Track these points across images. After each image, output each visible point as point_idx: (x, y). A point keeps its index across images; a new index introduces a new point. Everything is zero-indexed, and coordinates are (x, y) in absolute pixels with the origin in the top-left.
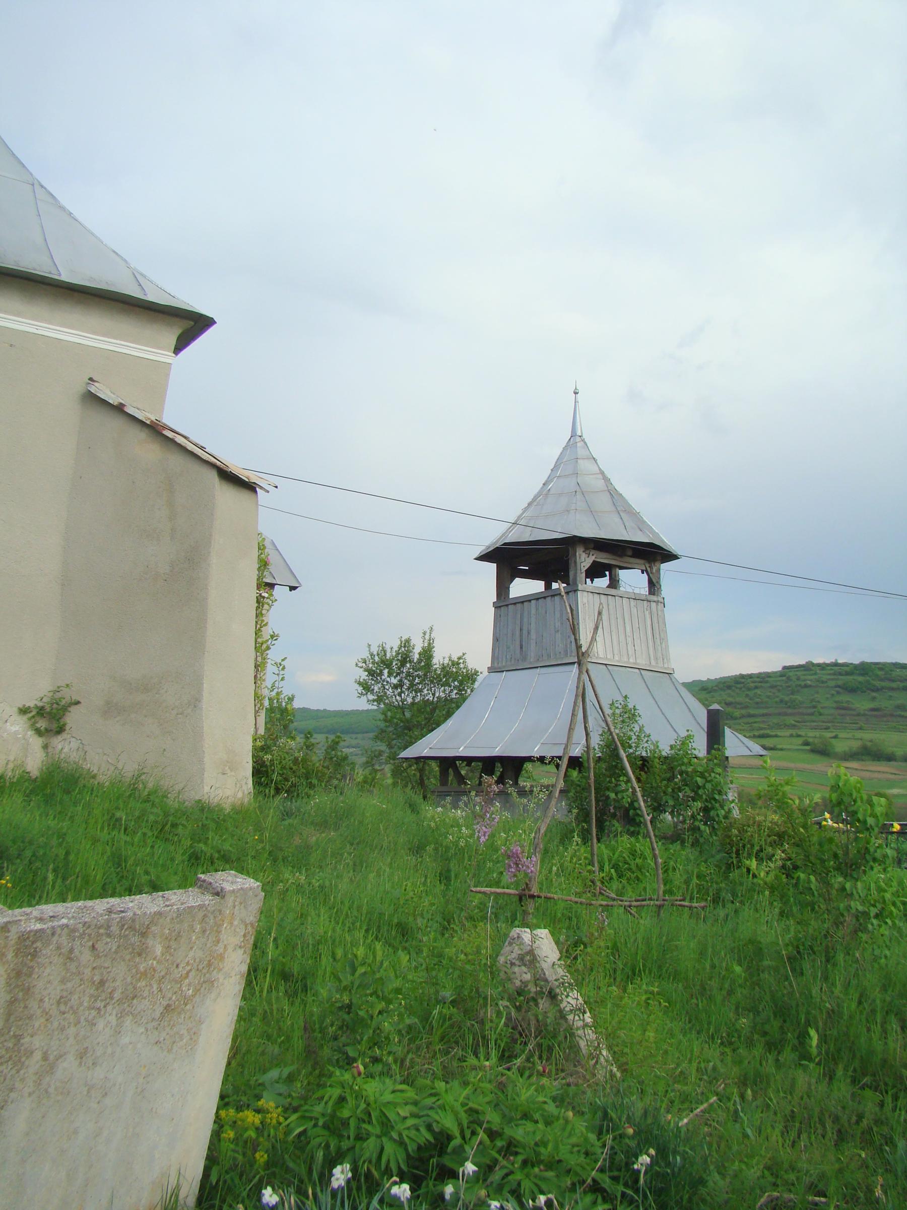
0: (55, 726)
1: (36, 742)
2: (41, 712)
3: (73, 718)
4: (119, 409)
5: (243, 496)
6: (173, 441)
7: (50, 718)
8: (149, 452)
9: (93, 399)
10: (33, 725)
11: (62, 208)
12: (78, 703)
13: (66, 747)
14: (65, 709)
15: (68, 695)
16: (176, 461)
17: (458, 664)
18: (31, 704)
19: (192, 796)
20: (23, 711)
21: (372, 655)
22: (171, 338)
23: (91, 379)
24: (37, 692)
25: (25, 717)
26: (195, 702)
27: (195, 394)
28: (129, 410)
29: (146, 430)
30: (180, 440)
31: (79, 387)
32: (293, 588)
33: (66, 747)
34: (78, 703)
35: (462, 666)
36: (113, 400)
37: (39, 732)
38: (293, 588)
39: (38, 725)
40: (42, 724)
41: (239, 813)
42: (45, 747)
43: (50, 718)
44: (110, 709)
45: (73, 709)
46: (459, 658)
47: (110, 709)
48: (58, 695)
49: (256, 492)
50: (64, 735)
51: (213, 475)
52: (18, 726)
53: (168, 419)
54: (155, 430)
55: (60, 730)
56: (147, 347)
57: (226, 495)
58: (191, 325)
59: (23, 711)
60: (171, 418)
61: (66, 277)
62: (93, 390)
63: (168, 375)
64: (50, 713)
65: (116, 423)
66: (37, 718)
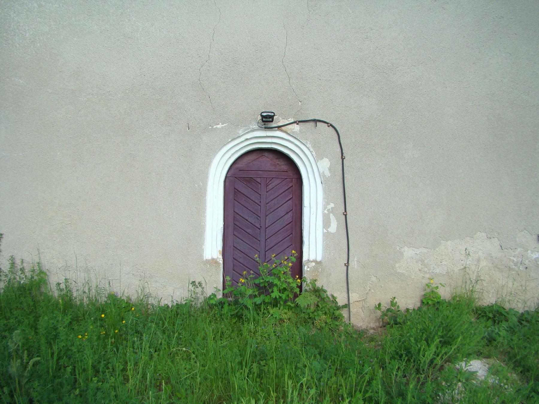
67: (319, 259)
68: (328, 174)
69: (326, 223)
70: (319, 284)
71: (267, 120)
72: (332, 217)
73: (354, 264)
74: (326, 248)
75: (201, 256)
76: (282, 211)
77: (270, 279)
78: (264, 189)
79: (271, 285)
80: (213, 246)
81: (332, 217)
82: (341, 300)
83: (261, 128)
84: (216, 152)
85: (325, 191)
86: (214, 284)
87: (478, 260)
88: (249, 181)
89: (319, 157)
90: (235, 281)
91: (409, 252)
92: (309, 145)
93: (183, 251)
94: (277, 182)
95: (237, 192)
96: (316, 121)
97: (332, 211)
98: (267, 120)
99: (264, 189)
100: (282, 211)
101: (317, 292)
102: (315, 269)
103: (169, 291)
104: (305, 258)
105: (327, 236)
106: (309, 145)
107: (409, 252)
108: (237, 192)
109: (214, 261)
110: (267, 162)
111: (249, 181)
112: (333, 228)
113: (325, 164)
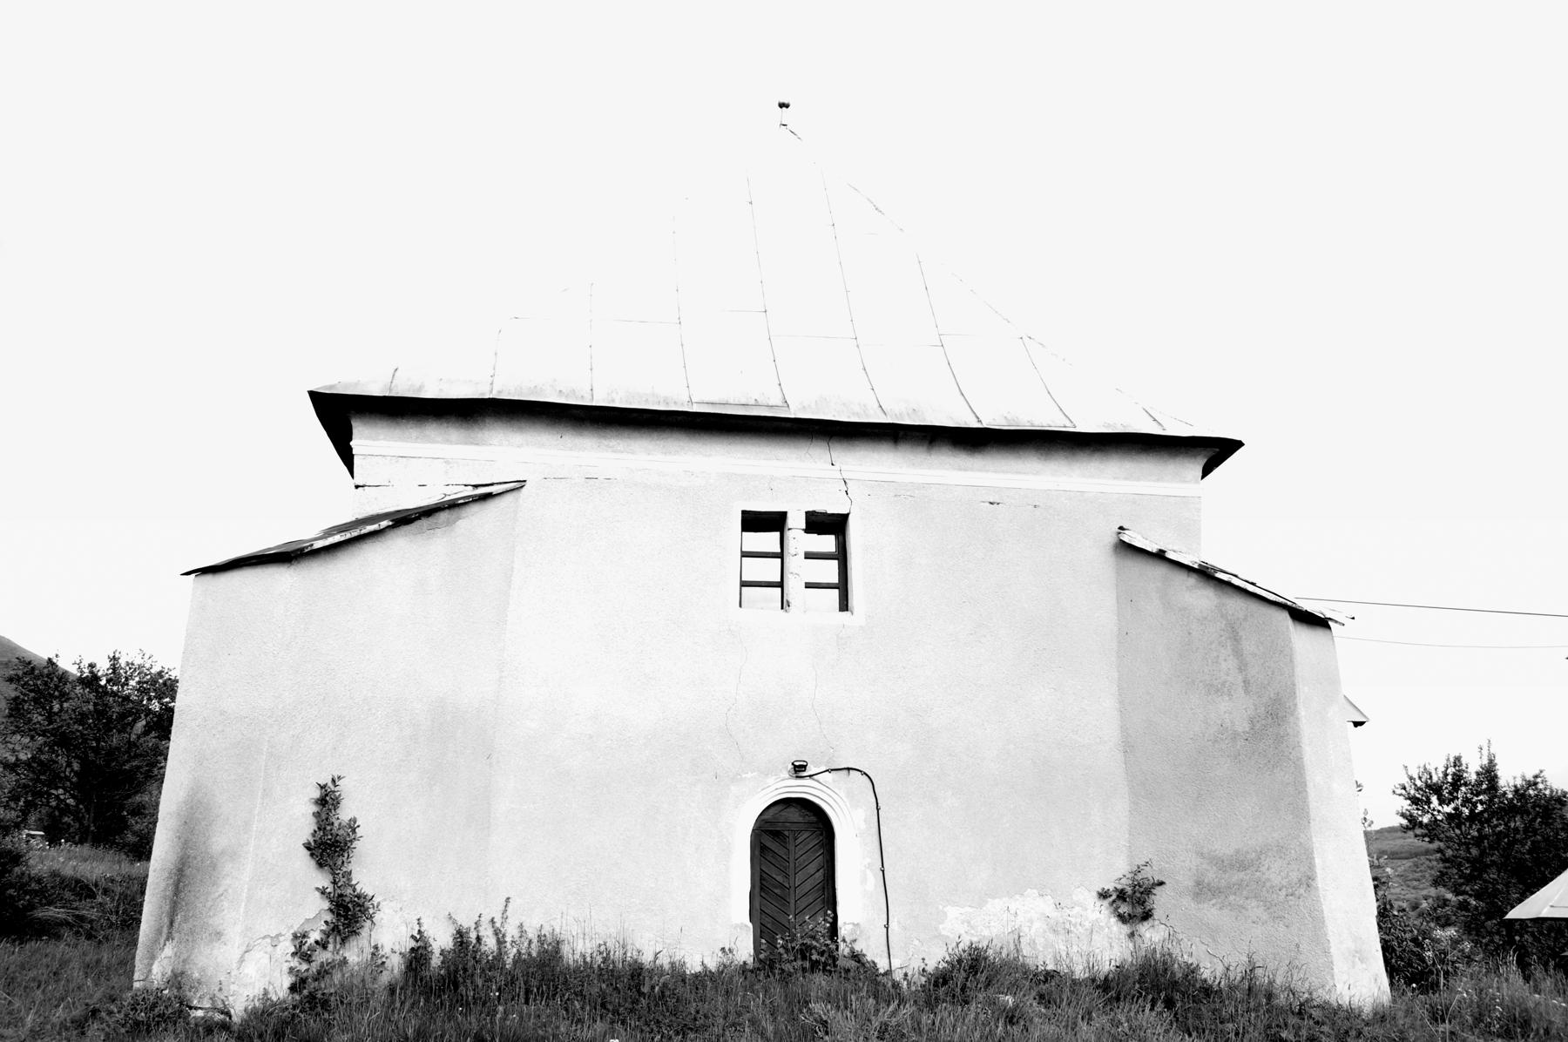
0: (1139, 910)
2: (1121, 895)
3: (1160, 901)
4: (1160, 556)
5: (1317, 634)
7: (1133, 902)
10: (1116, 909)
12: (1161, 883)
13: (1152, 935)
14: (1148, 892)
15: (1151, 874)
16: (1236, 604)
17: (1536, 784)
18: (1110, 886)
19: (1321, 995)
20: (1104, 895)
22: (1196, 467)
23: (1121, 528)
24: (1115, 874)
25: (1106, 903)
26: (1308, 881)
28: (1170, 555)
31: (1111, 539)
32: (1357, 724)
33: (1152, 935)
34: (1161, 883)
35: (1541, 786)
36: (1152, 548)
37: (1123, 918)
38: (1357, 724)
40: (1124, 909)
41: (1381, 1017)
43: (1133, 902)
44: (1202, 890)
45: (1157, 890)
47: (1202, 890)
48: (1139, 877)
49: (1329, 627)
51: (1285, 615)
53: (1213, 561)
54: (1205, 574)
55: (1147, 916)
56: (1177, 481)
57: (1302, 637)
58: (1215, 451)
59: (1104, 895)
62: (1126, 539)
64: (1131, 897)
65: (1160, 570)
66: (1119, 903)
69: (864, 880)
70: (858, 947)
71: (799, 769)
76: (812, 868)
77: (807, 941)
78: (793, 844)
79: (810, 948)
82: (882, 966)
86: (745, 951)
87: (1031, 921)
88: (777, 835)
90: (772, 944)
91: (952, 912)
92: (842, 794)
94: (806, 835)
99: (793, 844)
100: (812, 868)
101: (856, 957)
103: (698, 956)
106: (842, 794)
107: (952, 912)
109: (743, 926)
110: (794, 815)
111: (777, 835)
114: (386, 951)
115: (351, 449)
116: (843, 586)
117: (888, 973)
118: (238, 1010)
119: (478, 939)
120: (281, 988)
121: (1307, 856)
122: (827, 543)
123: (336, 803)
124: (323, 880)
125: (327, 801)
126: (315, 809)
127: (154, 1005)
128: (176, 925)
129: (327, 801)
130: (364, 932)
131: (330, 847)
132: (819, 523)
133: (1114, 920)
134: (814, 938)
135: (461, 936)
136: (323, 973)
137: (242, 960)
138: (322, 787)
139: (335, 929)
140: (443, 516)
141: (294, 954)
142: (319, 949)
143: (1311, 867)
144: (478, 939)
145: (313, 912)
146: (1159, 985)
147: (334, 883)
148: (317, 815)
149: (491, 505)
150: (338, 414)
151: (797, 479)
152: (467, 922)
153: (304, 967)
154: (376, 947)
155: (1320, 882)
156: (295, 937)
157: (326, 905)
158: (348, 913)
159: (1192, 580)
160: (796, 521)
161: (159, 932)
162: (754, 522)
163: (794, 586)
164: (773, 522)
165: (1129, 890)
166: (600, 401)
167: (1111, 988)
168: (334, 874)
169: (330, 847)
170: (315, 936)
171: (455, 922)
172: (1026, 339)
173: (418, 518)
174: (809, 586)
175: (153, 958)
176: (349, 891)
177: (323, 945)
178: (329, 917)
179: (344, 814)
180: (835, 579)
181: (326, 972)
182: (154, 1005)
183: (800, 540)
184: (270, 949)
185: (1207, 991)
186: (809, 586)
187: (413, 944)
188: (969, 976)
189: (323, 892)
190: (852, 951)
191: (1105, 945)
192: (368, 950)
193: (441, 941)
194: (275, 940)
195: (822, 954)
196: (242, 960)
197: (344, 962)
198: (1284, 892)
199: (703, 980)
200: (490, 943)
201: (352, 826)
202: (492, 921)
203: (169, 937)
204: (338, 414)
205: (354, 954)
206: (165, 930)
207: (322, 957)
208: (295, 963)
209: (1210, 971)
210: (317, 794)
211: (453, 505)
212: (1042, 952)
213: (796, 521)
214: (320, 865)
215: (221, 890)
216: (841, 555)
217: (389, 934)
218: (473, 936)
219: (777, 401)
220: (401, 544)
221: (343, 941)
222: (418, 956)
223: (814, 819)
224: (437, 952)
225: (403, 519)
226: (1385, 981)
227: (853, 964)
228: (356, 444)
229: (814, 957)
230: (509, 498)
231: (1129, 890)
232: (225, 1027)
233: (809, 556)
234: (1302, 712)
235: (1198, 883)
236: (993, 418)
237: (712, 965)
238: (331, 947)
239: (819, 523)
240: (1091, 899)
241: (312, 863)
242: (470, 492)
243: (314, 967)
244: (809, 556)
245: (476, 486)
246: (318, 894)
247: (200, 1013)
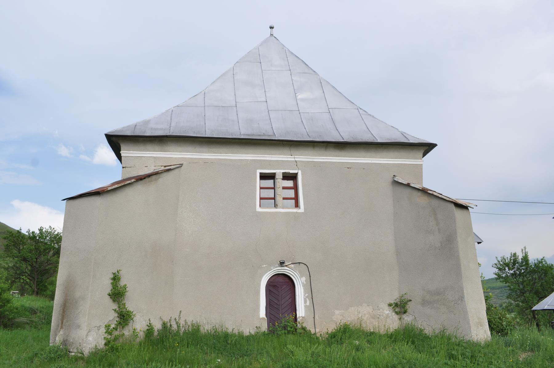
0: (403, 310)
1: (396, 317)
2: (396, 305)
3: (410, 307)
4: (408, 185)
5: (465, 211)
6: (433, 195)
7: (400, 307)
8: (423, 200)
9: (396, 183)
11: (370, 115)
12: (410, 300)
13: (408, 319)
14: (406, 303)
15: (407, 297)
16: (435, 202)
17: (542, 262)
18: (392, 302)
19: (467, 338)
20: (390, 305)
21: (499, 261)
23: (394, 176)
24: (394, 297)
26: (462, 298)
27: (434, 174)
28: (412, 185)
29: (420, 192)
30: (435, 194)
31: (390, 180)
32: (479, 243)
33: (408, 319)
34: (410, 300)
35: (544, 263)
36: (405, 182)
37: (397, 313)
39: (396, 310)
40: (397, 310)
41: (488, 345)
42: (400, 319)
43: (400, 307)
44: (425, 303)
45: (409, 303)
46: (542, 259)
48: (403, 298)
49: (468, 209)
50: (407, 314)
51: (453, 205)
52: (388, 311)
54: (424, 191)
55: (405, 312)
57: (459, 213)
58: (428, 147)
59: (390, 305)
60: (426, 184)
61: (379, 141)
63: (422, 169)
65: (408, 191)
67: (303, 316)
68: (305, 283)
69: (305, 302)
70: (304, 325)
72: (307, 299)
73: (316, 317)
74: (306, 311)
75: (259, 316)
77: (286, 323)
78: (281, 290)
80: (262, 313)
81: (307, 299)
82: (313, 331)
83: (279, 266)
84: (263, 276)
85: (304, 289)
86: (264, 327)
87: (365, 315)
88: (274, 286)
89: (301, 276)
90: (274, 325)
91: (337, 312)
93: (251, 314)
95: (270, 291)
96: (299, 263)
97: (307, 297)
98: (282, 264)
99: (281, 290)
101: (304, 329)
102: (302, 320)
103: (248, 330)
104: (298, 316)
105: (306, 306)
108: (270, 291)
109: (263, 318)
110: (281, 279)
112: (308, 303)
113: (304, 279)
114: (138, 330)
115: (120, 154)
116: (296, 198)
117: (315, 334)
118: (86, 352)
119: (171, 325)
120: (101, 344)
121: (461, 290)
122: (290, 183)
123: (119, 279)
124: (115, 306)
125: (116, 278)
126: (111, 281)
127: (57, 352)
128: (64, 323)
129: (116, 278)
130: (130, 324)
131: (117, 295)
132: (286, 177)
133: (393, 314)
134: (288, 322)
135: (164, 325)
136: (116, 339)
137: (87, 335)
138: (114, 274)
139: (120, 323)
140: (154, 177)
141: (106, 332)
142: (114, 330)
143: (463, 293)
144: (171, 325)
145: (112, 317)
146: (410, 336)
147: (119, 307)
148: (112, 284)
149: (171, 173)
150: (116, 142)
151: (279, 161)
152: (166, 319)
153: (109, 337)
154: (135, 329)
155: (466, 299)
156: (106, 326)
157: (116, 315)
158: (124, 317)
159: (419, 194)
160: (279, 176)
161: (58, 326)
162: (264, 177)
163: (279, 199)
164: (272, 177)
165: (399, 303)
166: (208, 135)
167: (393, 338)
168: (118, 304)
169: (117, 295)
170: (113, 326)
171: (162, 320)
172: (359, 110)
173: (145, 178)
174: (284, 199)
175: (56, 335)
176: (124, 310)
177: (116, 329)
178: (118, 319)
179: (122, 283)
180: (293, 196)
181: (117, 338)
182: (57, 352)
183: (281, 183)
184: (97, 331)
185: (427, 338)
186: (284, 199)
187: (148, 328)
188: (343, 334)
189: (115, 310)
190: (302, 326)
191: (391, 322)
192: (132, 330)
193: (157, 326)
194: (99, 328)
195: (291, 328)
196: (87, 335)
197: (123, 334)
198: (453, 303)
199: (250, 339)
200: (175, 327)
201: (125, 287)
202: (175, 319)
203: (62, 328)
204: (116, 142)
205: (127, 332)
206: (60, 325)
207: (116, 333)
208: (106, 335)
209: (428, 331)
210: (112, 276)
211: (156, 173)
212: (370, 325)
213: (279, 176)
214: (114, 301)
215: (79, 311)
216: (295, 188)
217: (139, 325)
218: (169, 324)
219: (271, 133)
220: (139, 187)
221: (123, 328)
222: (149, 332)
223: (288, 280)
224: (156, 330)
225: (140, 179)
226: (489, 333)
227: (302, 331)
228: (123, 153)
229: (289, 329)
230: (177, 170)
231: (399, 303)
232: (82, 358)
233: (284, 188)
234: (459, 239)
235: (423, 300)
236: (347, 138)
237: (253, 332)
238: (118, 330)
239: (286, 177)
240: (386, 307)
241: (111, 300)
242: (163, 168)
243: (113, 336)
244: (284, 188)
245: (165, 166)
246: (113, 311)
247: (73, 354)
